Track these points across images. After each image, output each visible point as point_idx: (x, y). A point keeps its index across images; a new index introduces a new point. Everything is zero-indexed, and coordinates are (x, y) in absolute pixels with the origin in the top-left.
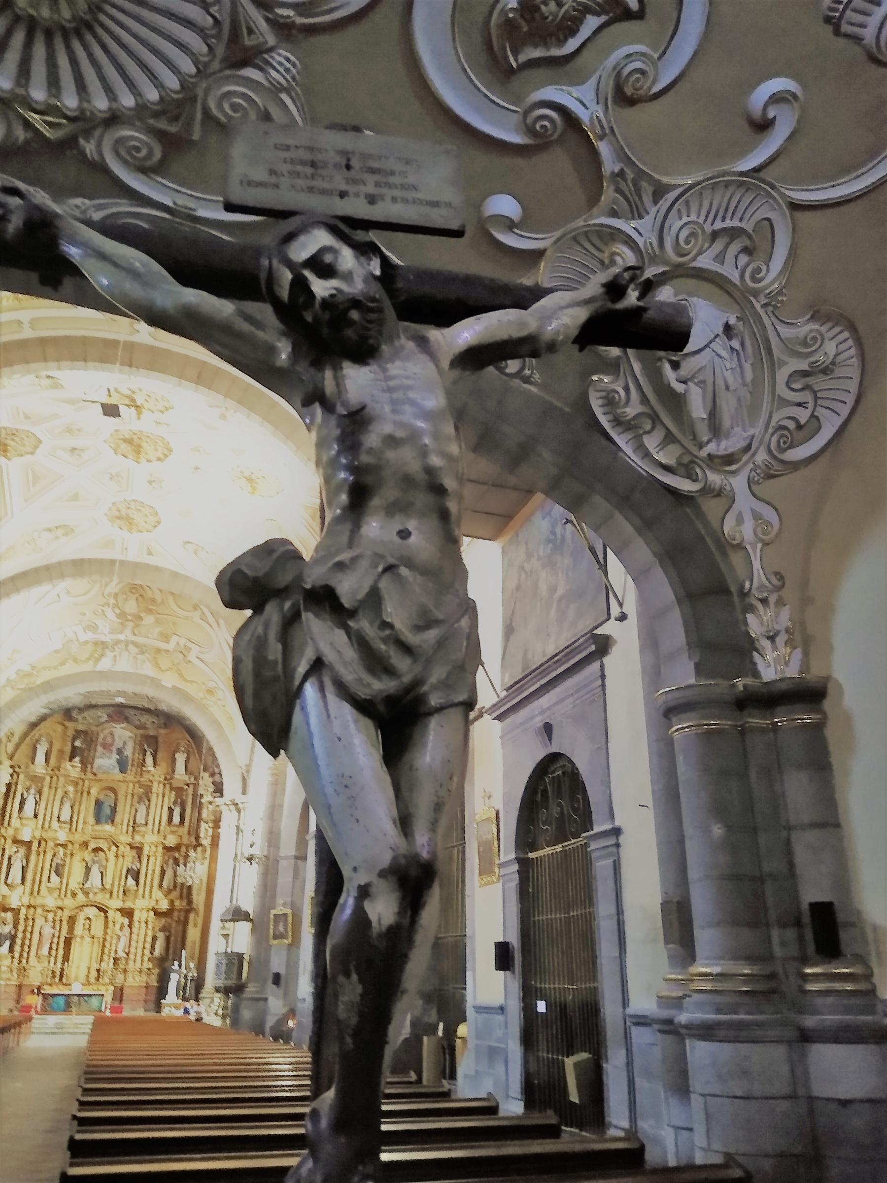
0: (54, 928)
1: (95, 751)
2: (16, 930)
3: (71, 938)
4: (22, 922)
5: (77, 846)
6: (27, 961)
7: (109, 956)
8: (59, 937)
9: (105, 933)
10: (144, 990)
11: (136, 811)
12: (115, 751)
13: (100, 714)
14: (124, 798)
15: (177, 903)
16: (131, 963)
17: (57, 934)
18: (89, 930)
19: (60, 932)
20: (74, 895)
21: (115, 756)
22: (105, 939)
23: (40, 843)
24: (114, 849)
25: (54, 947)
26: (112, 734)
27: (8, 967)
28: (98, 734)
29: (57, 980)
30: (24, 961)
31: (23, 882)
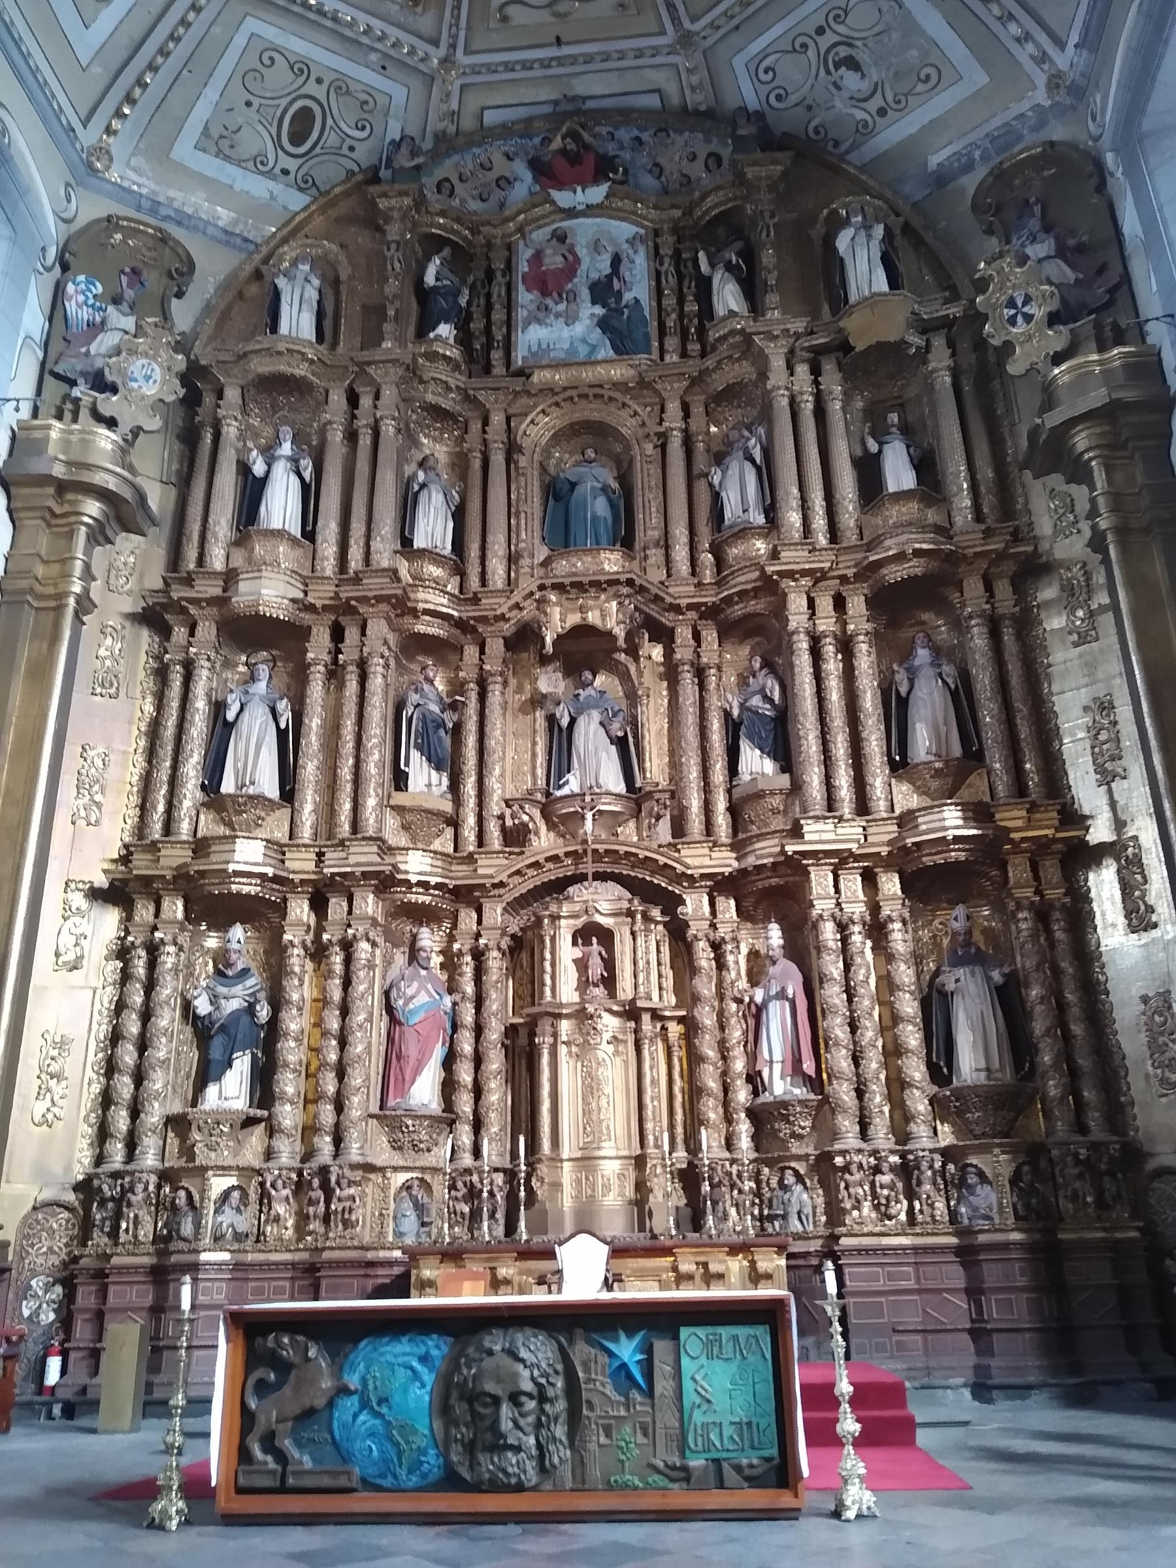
0: (452, 988)
1: (510, 306)
3: (532, 1027)
4: (297, 959)
5: (495, 647)
6: (338, 1141)
7: (726, 1104)
8: (479, 1030)
9: (687, 996)
10: (956, 1276)
11: (716, 497)
12: (585, 294)
13: (501, 166)
14: (655, 470)
15: (1012, 818)
16: (848, 1125)
18: (609, 982)
19: (479, 1002)
20: (516, 837)
21: (590, 312)
22: (691, 1026)
23: (338, 634)
24: (657, 652)
25: (465, 1074)
26: (561, 237)
27: (246, 1172)
28: (509, 247)
29: (490, 1230)
30: (325, 1143)
31: (289, 794)
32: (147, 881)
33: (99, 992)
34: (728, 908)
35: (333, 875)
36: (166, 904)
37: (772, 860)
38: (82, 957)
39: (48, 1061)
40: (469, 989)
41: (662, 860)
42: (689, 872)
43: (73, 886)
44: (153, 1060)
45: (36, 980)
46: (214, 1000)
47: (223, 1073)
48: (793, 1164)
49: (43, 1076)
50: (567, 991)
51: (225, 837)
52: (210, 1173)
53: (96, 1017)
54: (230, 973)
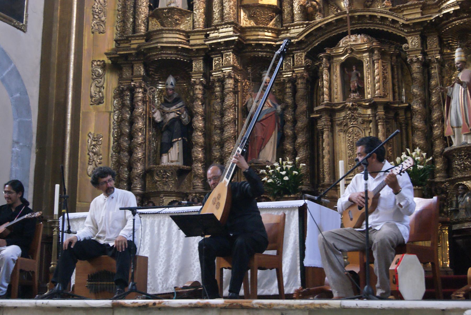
2: (192, 115)
17: (289, 117)
18: (361, 90)
32: (125, 57)
33: (112, 114)
34: (433, 42)
35: (211, 45)
36: (135, 68)
37: (453, 9)
38: (103, 98)
39: (92, 147)
40: (289, 101)
41: (390, 17)
42: (405, 23)
43: (95, 63)
44: (135, 144)
45: (82, 109)
46: (163, 114)
47: (169, 149)
48: (464, 182)
49: (91, 154)
50: (338, 97)
51: (160, 30)
52: (162, 195)
53: (112, 126)
54: (170, 101)
